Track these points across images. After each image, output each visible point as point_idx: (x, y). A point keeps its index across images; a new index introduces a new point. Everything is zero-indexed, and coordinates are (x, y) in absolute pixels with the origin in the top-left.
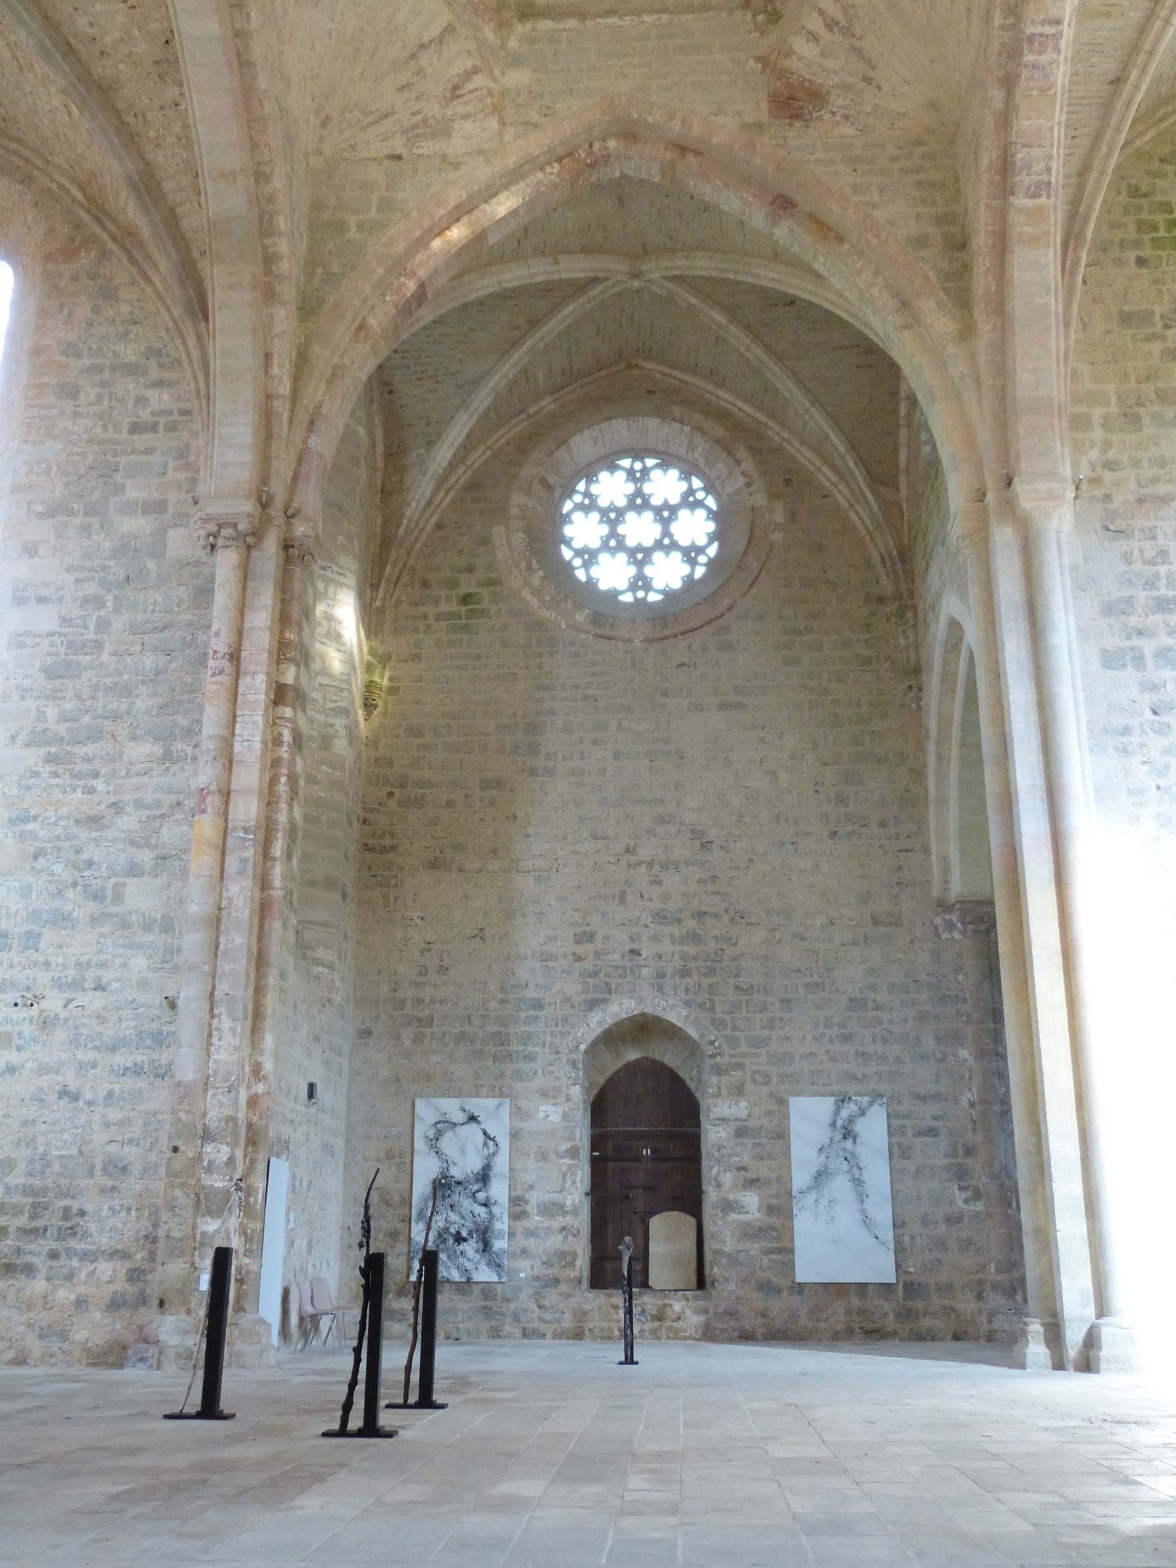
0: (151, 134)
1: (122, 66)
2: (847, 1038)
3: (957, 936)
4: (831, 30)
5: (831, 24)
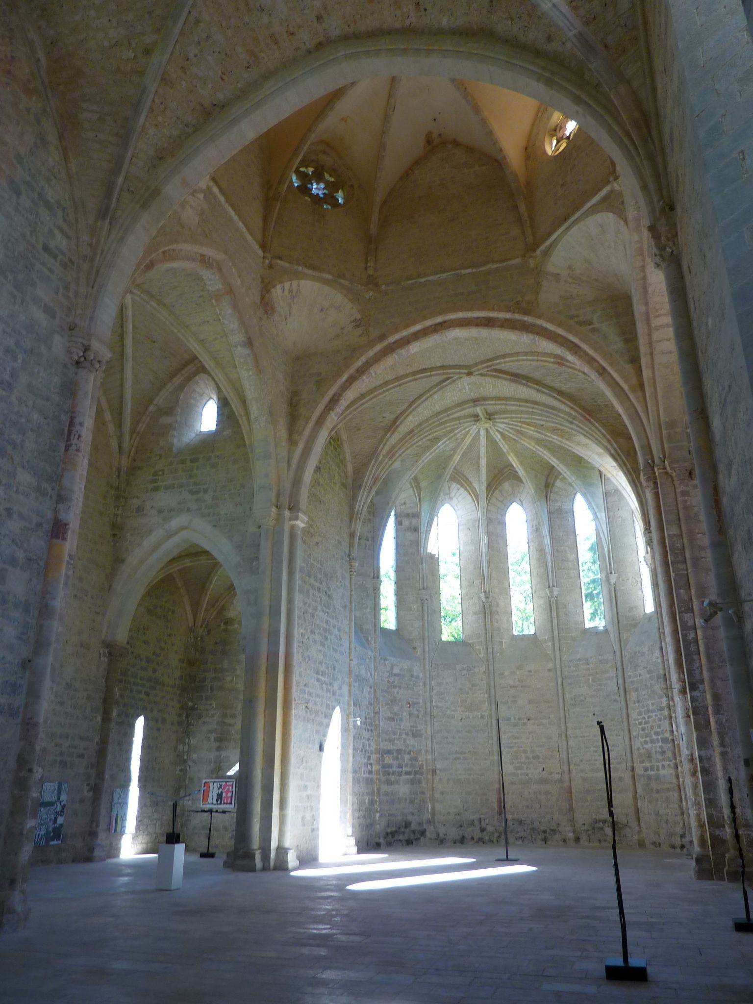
0: (160, 119)
1: (183, 83)
2: (62, 703)
3: (106, 660)
5: (290, 291)
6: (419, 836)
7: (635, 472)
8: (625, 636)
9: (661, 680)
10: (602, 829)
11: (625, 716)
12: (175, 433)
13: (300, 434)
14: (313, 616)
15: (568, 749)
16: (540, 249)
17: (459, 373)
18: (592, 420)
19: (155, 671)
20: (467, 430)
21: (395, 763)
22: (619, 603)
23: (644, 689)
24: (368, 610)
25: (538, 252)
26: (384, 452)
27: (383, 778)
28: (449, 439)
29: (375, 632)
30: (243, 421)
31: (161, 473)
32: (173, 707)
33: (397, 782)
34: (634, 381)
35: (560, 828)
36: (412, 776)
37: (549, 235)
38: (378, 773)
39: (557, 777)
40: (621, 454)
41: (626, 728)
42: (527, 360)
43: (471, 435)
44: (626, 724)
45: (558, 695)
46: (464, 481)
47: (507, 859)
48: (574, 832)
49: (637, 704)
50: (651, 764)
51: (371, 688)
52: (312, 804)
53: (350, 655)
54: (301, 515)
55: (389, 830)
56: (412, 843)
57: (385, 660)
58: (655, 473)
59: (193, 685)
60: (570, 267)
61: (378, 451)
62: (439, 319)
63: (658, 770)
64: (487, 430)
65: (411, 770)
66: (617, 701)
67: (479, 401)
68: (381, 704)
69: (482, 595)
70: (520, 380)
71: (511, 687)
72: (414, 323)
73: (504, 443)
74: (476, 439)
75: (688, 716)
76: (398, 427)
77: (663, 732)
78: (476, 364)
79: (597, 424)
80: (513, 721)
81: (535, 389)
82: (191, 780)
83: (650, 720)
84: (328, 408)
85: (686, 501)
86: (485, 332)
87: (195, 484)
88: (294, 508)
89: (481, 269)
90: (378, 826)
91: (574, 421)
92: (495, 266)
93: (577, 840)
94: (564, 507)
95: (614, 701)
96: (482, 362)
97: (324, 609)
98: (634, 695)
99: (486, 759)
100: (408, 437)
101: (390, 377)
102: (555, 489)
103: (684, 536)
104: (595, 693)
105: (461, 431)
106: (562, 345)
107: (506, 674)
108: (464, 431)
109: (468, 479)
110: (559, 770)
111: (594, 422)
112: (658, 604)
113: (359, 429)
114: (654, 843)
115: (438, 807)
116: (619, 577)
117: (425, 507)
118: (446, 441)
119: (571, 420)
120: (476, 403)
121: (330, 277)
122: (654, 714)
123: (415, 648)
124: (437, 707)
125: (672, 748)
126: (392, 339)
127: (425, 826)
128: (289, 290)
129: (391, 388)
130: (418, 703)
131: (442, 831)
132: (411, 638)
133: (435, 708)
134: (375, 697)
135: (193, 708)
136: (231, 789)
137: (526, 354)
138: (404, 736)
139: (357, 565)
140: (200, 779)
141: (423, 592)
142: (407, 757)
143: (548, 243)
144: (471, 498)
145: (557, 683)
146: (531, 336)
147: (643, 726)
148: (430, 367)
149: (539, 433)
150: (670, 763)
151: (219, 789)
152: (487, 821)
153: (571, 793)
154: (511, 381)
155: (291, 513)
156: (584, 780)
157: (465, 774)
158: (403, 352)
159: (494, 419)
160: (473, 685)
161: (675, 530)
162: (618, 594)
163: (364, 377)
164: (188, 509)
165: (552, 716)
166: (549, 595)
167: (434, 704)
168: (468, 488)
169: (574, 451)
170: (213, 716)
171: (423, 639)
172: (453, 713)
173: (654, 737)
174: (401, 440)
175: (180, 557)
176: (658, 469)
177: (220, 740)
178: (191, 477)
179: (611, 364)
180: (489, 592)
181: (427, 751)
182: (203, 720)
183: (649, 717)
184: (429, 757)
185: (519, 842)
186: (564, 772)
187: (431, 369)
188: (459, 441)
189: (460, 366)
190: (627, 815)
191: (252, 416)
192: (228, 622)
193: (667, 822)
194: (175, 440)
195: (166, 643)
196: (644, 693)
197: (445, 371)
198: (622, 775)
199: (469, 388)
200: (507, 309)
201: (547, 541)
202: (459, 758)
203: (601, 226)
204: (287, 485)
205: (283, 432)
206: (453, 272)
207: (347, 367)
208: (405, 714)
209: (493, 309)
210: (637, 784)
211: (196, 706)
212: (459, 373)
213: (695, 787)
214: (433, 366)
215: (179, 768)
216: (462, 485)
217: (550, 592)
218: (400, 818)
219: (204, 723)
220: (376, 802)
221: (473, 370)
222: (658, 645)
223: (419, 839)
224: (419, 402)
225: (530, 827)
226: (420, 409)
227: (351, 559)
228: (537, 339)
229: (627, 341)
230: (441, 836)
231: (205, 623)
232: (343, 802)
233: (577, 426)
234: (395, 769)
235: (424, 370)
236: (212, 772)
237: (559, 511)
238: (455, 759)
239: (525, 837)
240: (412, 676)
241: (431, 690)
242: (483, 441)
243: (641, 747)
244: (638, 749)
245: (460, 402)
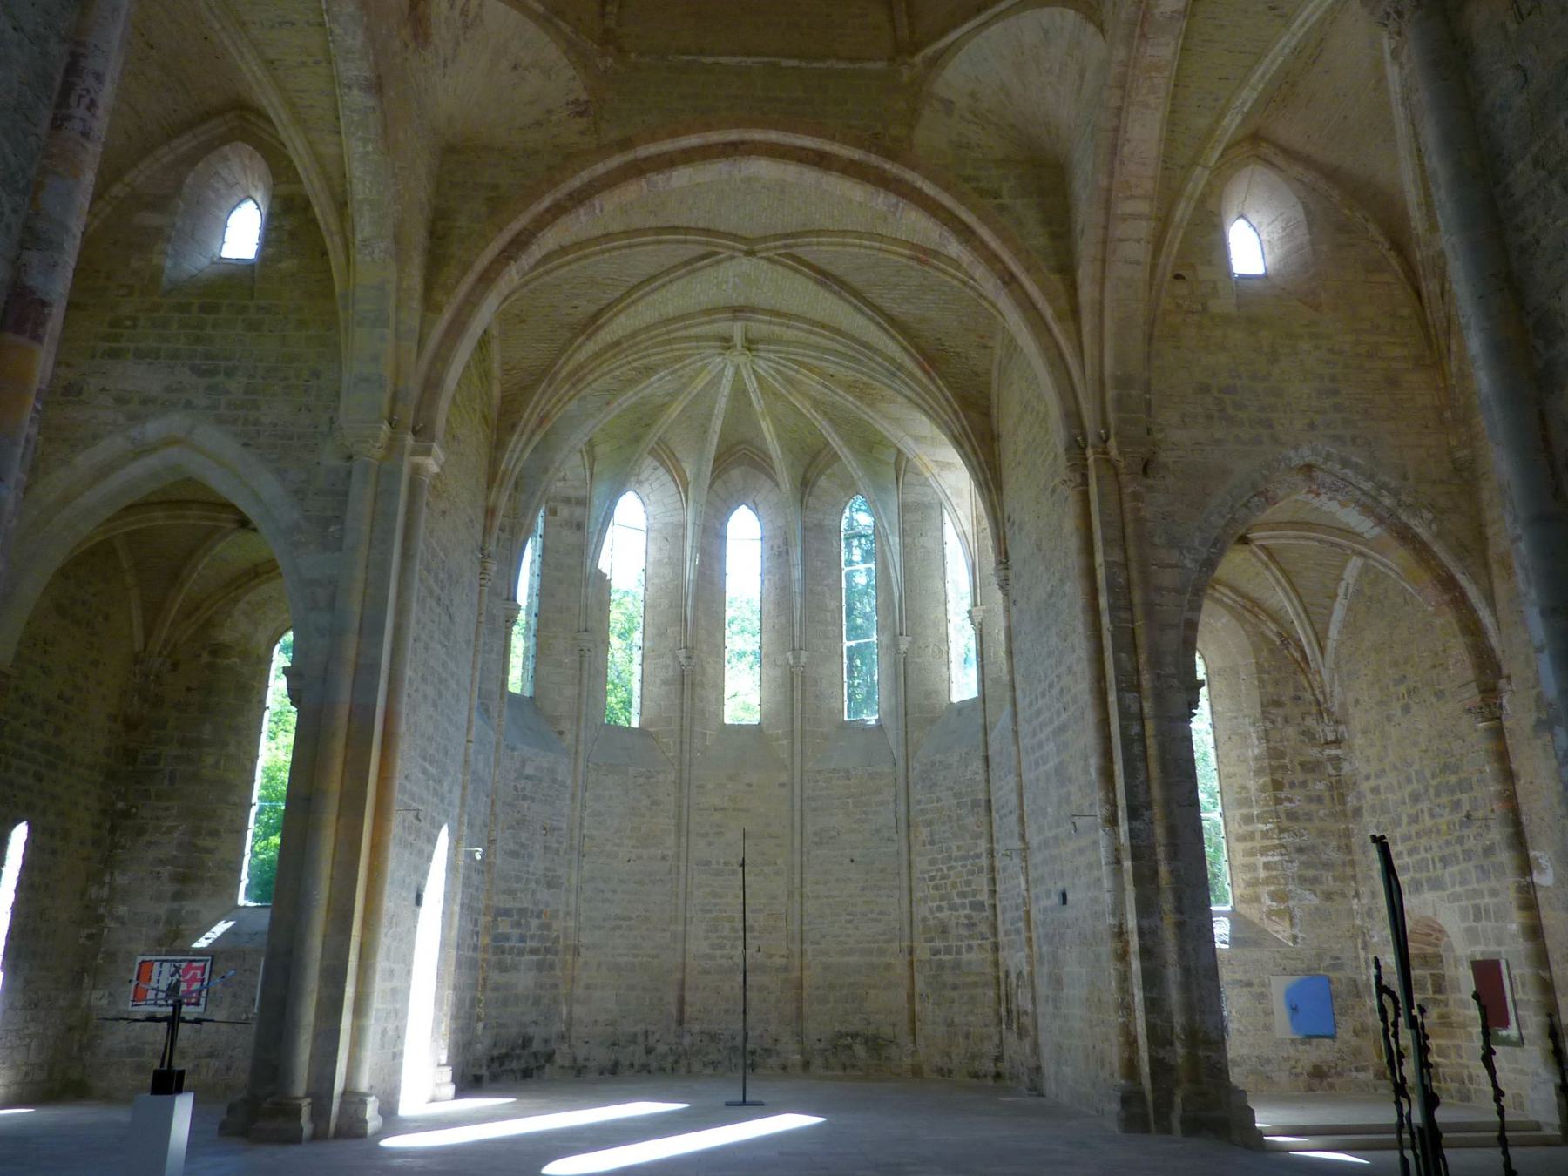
4: (461, 14)
5: (464, 12)
6: (542, 1061)
7: (990, 470)
9: (982, 810)
10: (850, 1047)
11: (905, 864)
12: (170, 251)
14: (426, 648)
15: (802, 916)
16: (922, 54)
17: (733, 249)
18: (933, 374)
19: (58, 731)
20: (706, 361)
21: (515, 932)
22: (909, 682)
23: (944, 823)
24: (494, 656)
25: (918, 59)
26: (564, 373)
27: (494, 959)
28: (671, 373)
29: (501, 697)
30: (333, 244)
31: (128, 323)
32: (87, 809)
33: (514, 967)
35: (778, 1047)
36: (540, 957)
37: (942, 33)
38: (485, 950)
40: (972, 436)
41: (905, 885)
42: (860, 246)
43: (709, 372)
44: (905, 877)
45: (793, 826)
46: (667, 456)
47: (744, 1103)
48: (802, 1054)
49: (928, 847)
50: (946, 944)
51: (487, 796)
52: (398, 1006)
53: (468, 730)
54: (436, 448)
55: (495, 1053)
56: (531, 1076)
57: (513, 749)
58: (1086, 459)
59: (130, 768)
60: (972, 95)
61: (556, 368)
62: (733, 135)
63: (959, 952)
64: (737, 368)
65: (539, 945)
66: (893, 841)
67: (742, 311)
68: (500, 826)
69: (682, 654)
70: (829, 283)
71: (715, 810)
72: (689, 131)
73: (760, 395)
74: (715, 382)
75: (1118, 862)
76: (600, 328)
77: (974, 893)
78: (765, 239)
79: (940, 382)
80: (714, 866)
81: (850, 303)
82: (111, 956)
83: (952, 872)
84: (506, 254)
85: (1139, 510)
86: (811, 175)
87: (207, 356)
88: (423, 432)
89: (816, 65)
90: (479, 1046)
91: (899, 373)
92: (842, 65)
93: (806, 1065)
94: (826, 522)
95: (888, 840)
96: (777, 237)
97: (442, 638)
98: (924, 833)
99: (664, 930)
100: (609, 355)
101: (616, 227)
103: (1133, 565)
104: (856, 826)
105: (695, 362)
106: (946, 225)
107: (710, 786)
108: (700, 364)
109: (674, 454)
110: (785, 951)
111: (937, 378)
113: (524, 321)
114: (940, 1071)
115: (579, 1011)
116: (913, 643)
117: (600, 490)
118: (666, 376)
119: (893, 369)
120: (737, 314)
121: (541, 9)
122: (960, 863)
123: (561, 733)
124: (591, 837)
125: (991, 918)
126: (643, 151)
127: (554, 1045)
128: (462, 10)
129: (615, 249)
130: (561, 829)
132: (555, 714)
133: (586, 839)
134: (493, 814)
135: (125, 814)
136: (199, 976)
137: (860, 235)
138: (533, 885)
139: (495, 568)
140: (130, 956)
141: (584, 635)
142: (534, 922)
143: (942, 44)
144: (675, 489)
145: (793, 807)
146: (893, 199)
147: (936, 882)
148: (685, 225)
149: (826, 387)
150: (984, 942)
151: (172, 975)
152: (657, 1036)
153: (800, 987)
154: (817, 282)
155: (416, 441)
156: (826, 968)
157: (627, 955)
158: (658, 179)
159: (757, 350)
160: (654, 803)
161: (1116, 556)
162: (910, 669)
163: (582, 211)
164: (188, 405)
165: (779, 861)
166: (791, 662)
167: (585, 831)
168: (671, 468)
169: (877, 426)
170: (170, 831)
171: (578, 719)
172: (616, 849)
173: (957, 901)
174: (597, 355)
175: (145, 505)
176: (1095, 453)
177: (182, 879)
178: (198, 340)
179: (1028, 270)
180: (693, 648)
181: (568, 914)
182: (146, 838)
183: (950, 868)
184: (571, 924)
185: (709, 1071)
186: (793, 956)
187: (687, 230)
188: (683, 380)
189: (735, 236)
190: (894, 1025)
191: (359, 237)
192: (217, 650)
193: (967, 1036)
194: (168, 263)
195: (86, 678)
196: (943, 828)
197: (710, 239)
198: (892, 961)
199: (735, 283)
200: (858, 143)
201: (797, 573)
202: (619, 928)
203: (1046, 32)
204: (414, 385)
205: (415, 280)
206: (766, 59)
207: (553, 184)
208: (537, 846)
209: (832, 138)
210: (916, 974)
211: (134, 810)
212: (733, 249)
214: (693, 225)
215: (87, 931)
216: (663, 463)
217: (794, 658)
218: (514, 1030)
219: (150, 844)
220: (480, 1001)
221: (757, 248)
222: (981, 753)
223: (544, 1066)
224: (647, 289)
225: (729, 1045)
226: (641, 306)
227: (485, 556)
228: (901, 205)
229: (1054, 236)
230: (580, 1060)
231: (168, 648)
232: (438, 1001)
233: (903, 381)
234: (514, 943)
235: (675, 229)
236: (160, 942)
237: (819, 526)
238: (613, 929)
239: (719, 1062)
240: (554, 781)
241: (584, 807)
242: (726, 386)
243: (930, 917)
244: (924, 920)
245: (710, 306)
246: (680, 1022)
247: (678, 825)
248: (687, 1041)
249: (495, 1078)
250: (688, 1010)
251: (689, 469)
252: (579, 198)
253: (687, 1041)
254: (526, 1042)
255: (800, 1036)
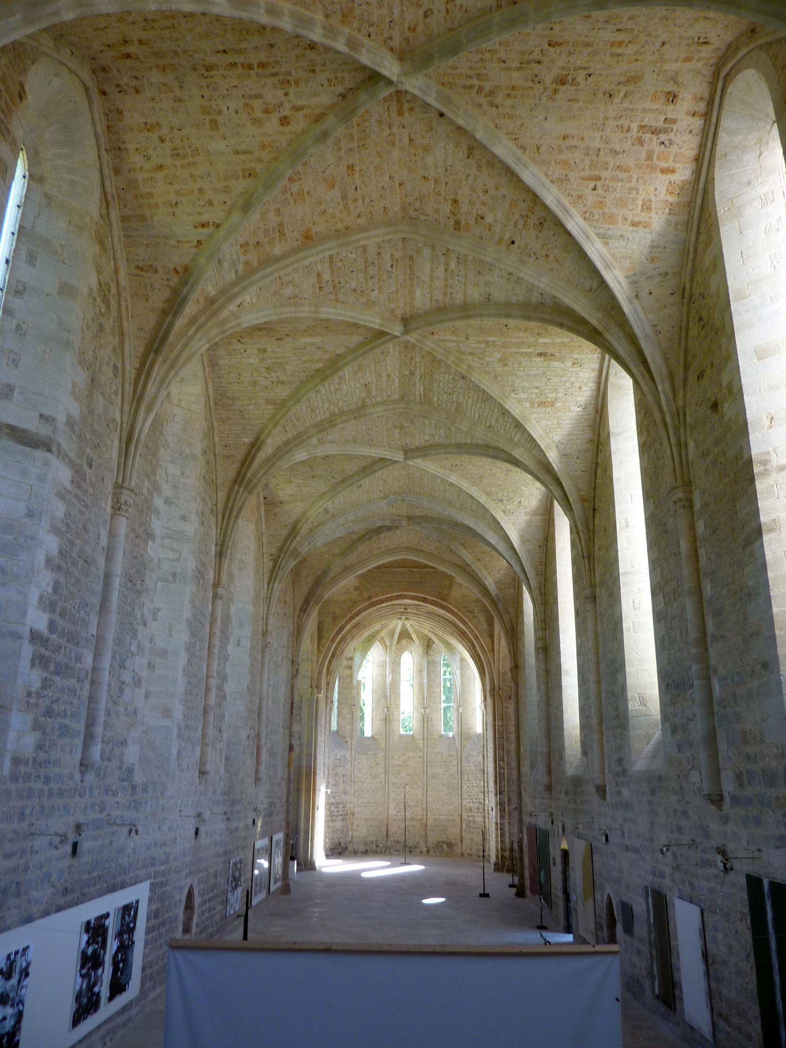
8: (464, 743)
13: (324, 647)
21: (335, 810)
33: (336, 821)
34: (490, 646)
39: (419, 817)
48: (427, 847)
62: (400, 593)
69: (386, 710)
72: (387, 593)
93: (428, 851)
94: (436, 660)
98: (466, 776)
102: (432, 649)
107: (396, 757)
112: (485, 729)
114: (469, 855)
115: (355, 834)
117: (357, 656)
123: (346, 742)
126: (374, 600)
131: (356, 847)
141: (353, 707)
142: (341, 806)
153: (426, 826)
156: (434, 819)
161: (500, 723)
185: (397, 853)
200: (435, 596)
201: (425, 680)
207: (350, 612)
213: (497, 835)
234: (336, 813)
237: (433, 662)
246: (387, 837)
247: (385, 771)
248: (389, 843)
249: (332, 855)
250: (389, 833)
251: (388, 643)
252: (357, 614)
253: (389, 843)
254: (340, 844)
255: (426, 842)
